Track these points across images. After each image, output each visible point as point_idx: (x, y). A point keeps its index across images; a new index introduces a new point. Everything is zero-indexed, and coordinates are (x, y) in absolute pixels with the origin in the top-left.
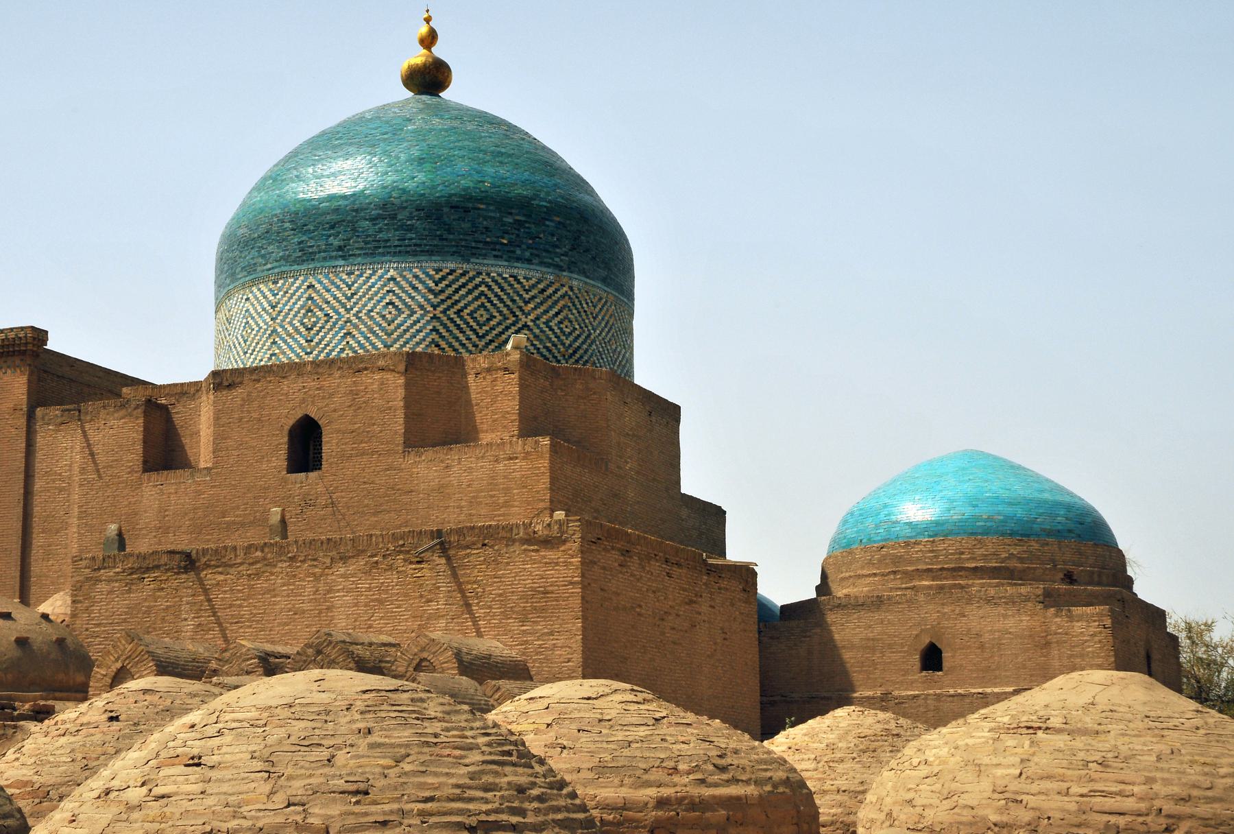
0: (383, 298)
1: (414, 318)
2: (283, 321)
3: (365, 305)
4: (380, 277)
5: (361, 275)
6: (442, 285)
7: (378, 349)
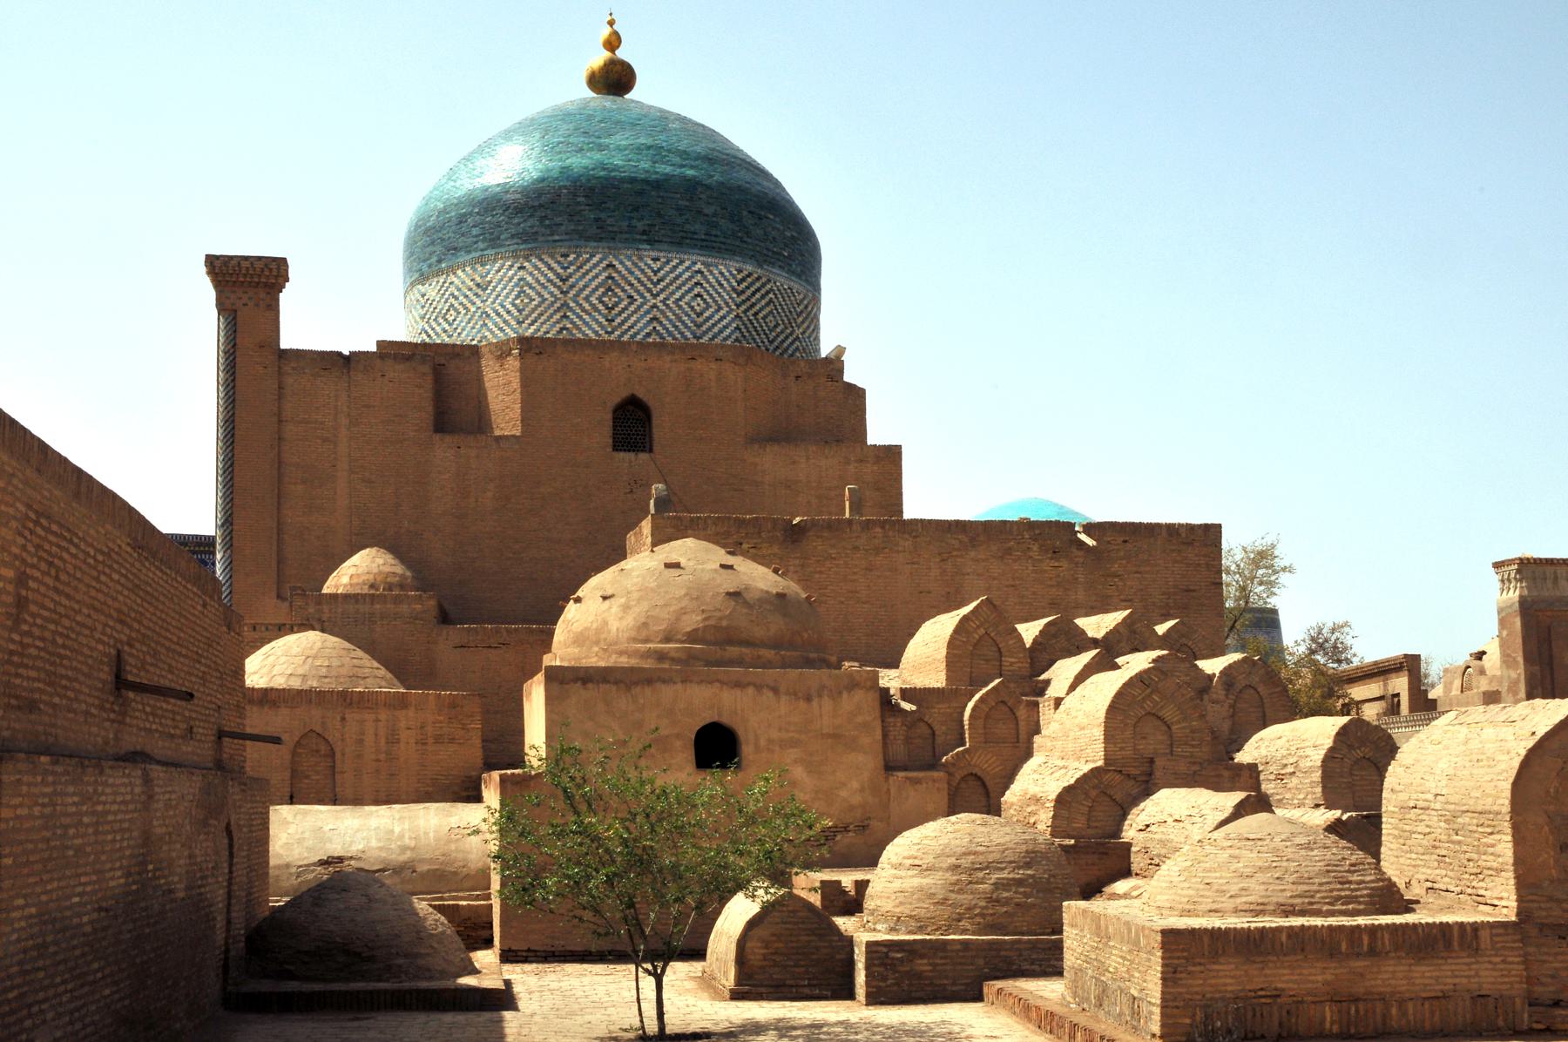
0: (691, 290)
1: (721, 313)
2: (577, 295)
3: (673, 293)
4: (688, 268)
5: (668, 262)
6: (745, 284)
7: (686, 338)
